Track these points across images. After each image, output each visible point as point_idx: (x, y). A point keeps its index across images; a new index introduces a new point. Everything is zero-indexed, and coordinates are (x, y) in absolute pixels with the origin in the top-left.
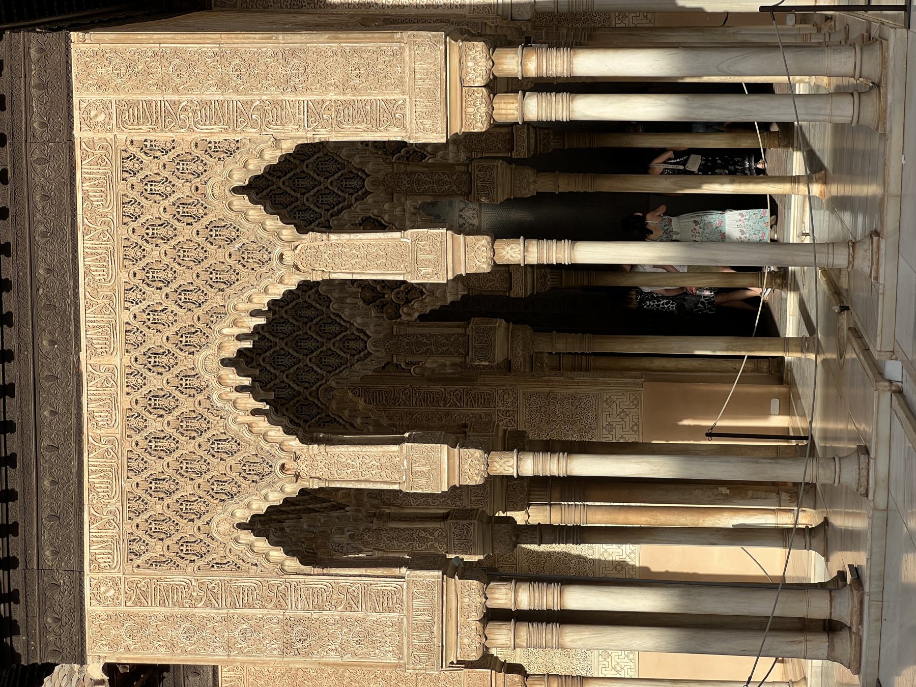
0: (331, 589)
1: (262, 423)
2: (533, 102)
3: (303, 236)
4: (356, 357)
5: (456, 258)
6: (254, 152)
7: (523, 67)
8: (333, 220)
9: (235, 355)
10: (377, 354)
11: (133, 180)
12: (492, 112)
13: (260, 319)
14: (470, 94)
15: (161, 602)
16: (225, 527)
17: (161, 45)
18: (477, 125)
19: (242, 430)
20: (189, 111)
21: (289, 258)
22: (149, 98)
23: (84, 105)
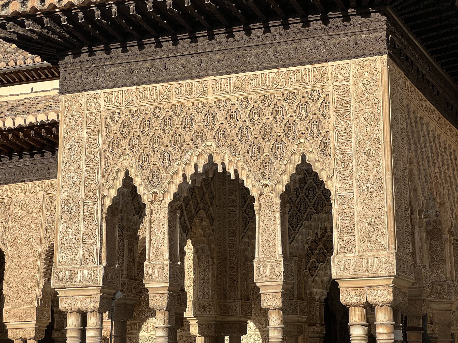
0: (94, 224)
1: (179, 180)
3: (278, 197)
5: (269, 287)
6: (324, 165)
7: (380, 325)
9: (214, 162)
11: (306, 96)
12: (352, 306)
14: (362, 292)
15: (89, 132)
16: (126, 163)
17: (382, 107)
18: (344, 297)
19: (174, 169)
20: (346, 126)
21: (267, 189)
22: (352, 102)
23: (346, 66)
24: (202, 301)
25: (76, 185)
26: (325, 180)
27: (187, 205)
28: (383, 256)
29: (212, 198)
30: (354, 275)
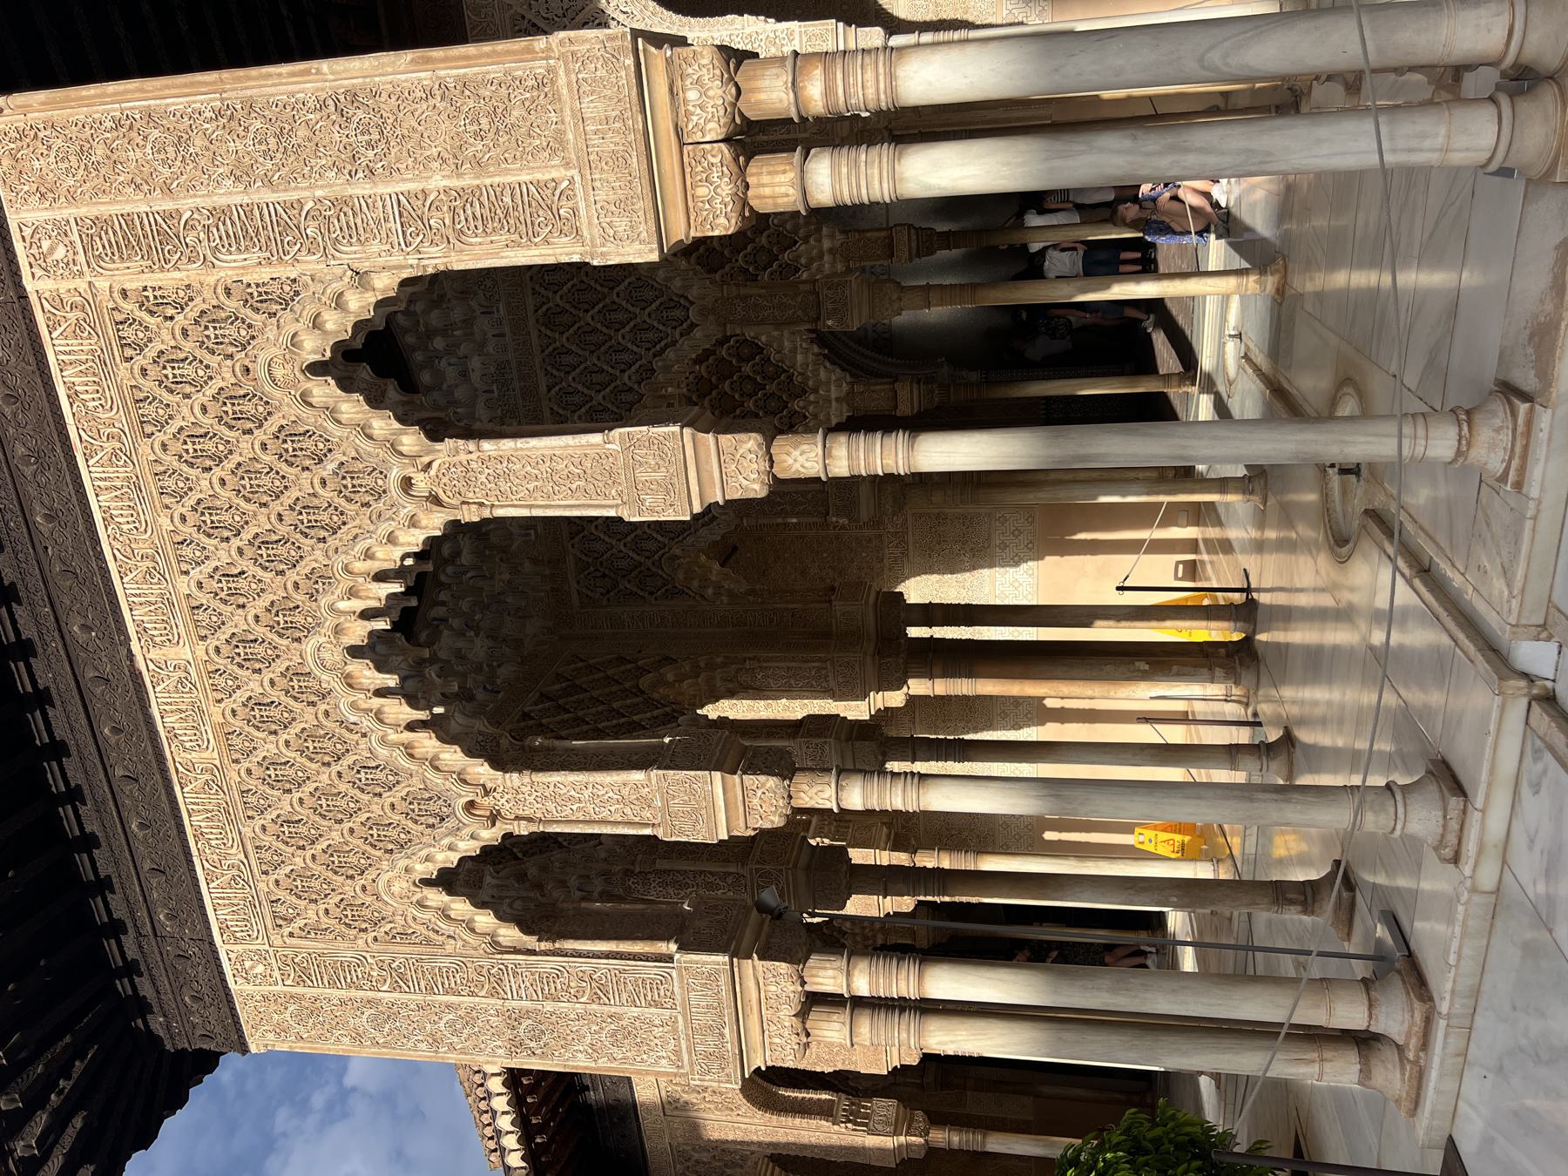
0: (566, 975)
1: (427, 743)
2: (823, 166)
3: (438, 446)
4: (700, 521)
5: (705, 475)
6: (324, 299)
7: (799, 94)
8: (657, 362)
9: (366, 641)
10: (723, 517)
12: (745, 194)
13: (393, 585)
14: (698, 158)
17: (123, 105)
18: (717, 221)
19: (394, 754)
20: (199, 228)
21: (421, 483)
22: (127, 209)
23: (27, 232)
24: (832, 683)
25: (470, 1018)
26: (372, 298)
27: (619, 713)
28: (574, 78)
29: (622, 660)
30: (643, 181)
